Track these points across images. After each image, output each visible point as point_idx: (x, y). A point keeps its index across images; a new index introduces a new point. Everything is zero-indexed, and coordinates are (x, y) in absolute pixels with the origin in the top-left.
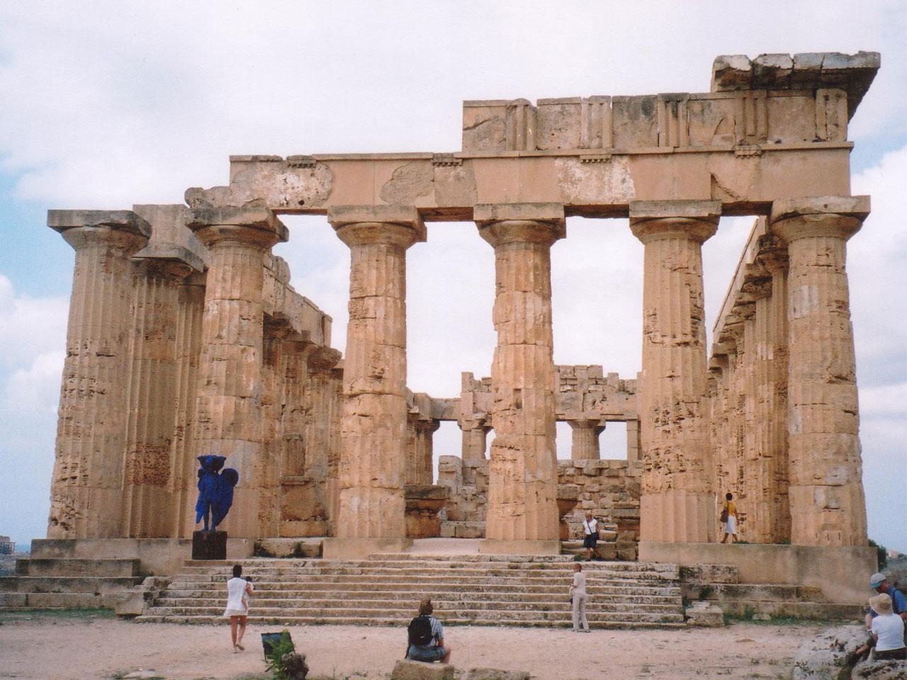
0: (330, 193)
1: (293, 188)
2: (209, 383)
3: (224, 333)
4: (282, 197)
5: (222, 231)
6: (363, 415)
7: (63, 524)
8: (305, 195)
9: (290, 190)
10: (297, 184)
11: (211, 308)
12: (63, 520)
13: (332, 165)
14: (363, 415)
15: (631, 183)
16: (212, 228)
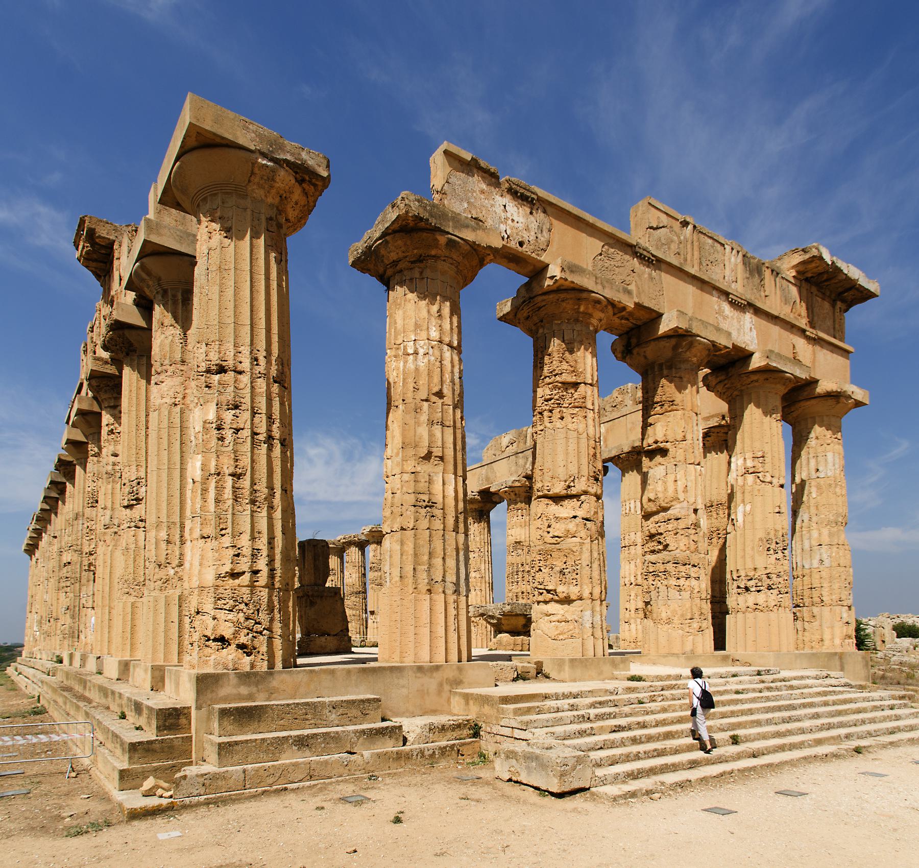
1: (513, 220)
4: (503, 227)
5: (451, 244)
6: (587, 520)
7: (241, 647)
8: (525, 236)
9: (510, 222)
12: (243, 639)
14: (587, 520)
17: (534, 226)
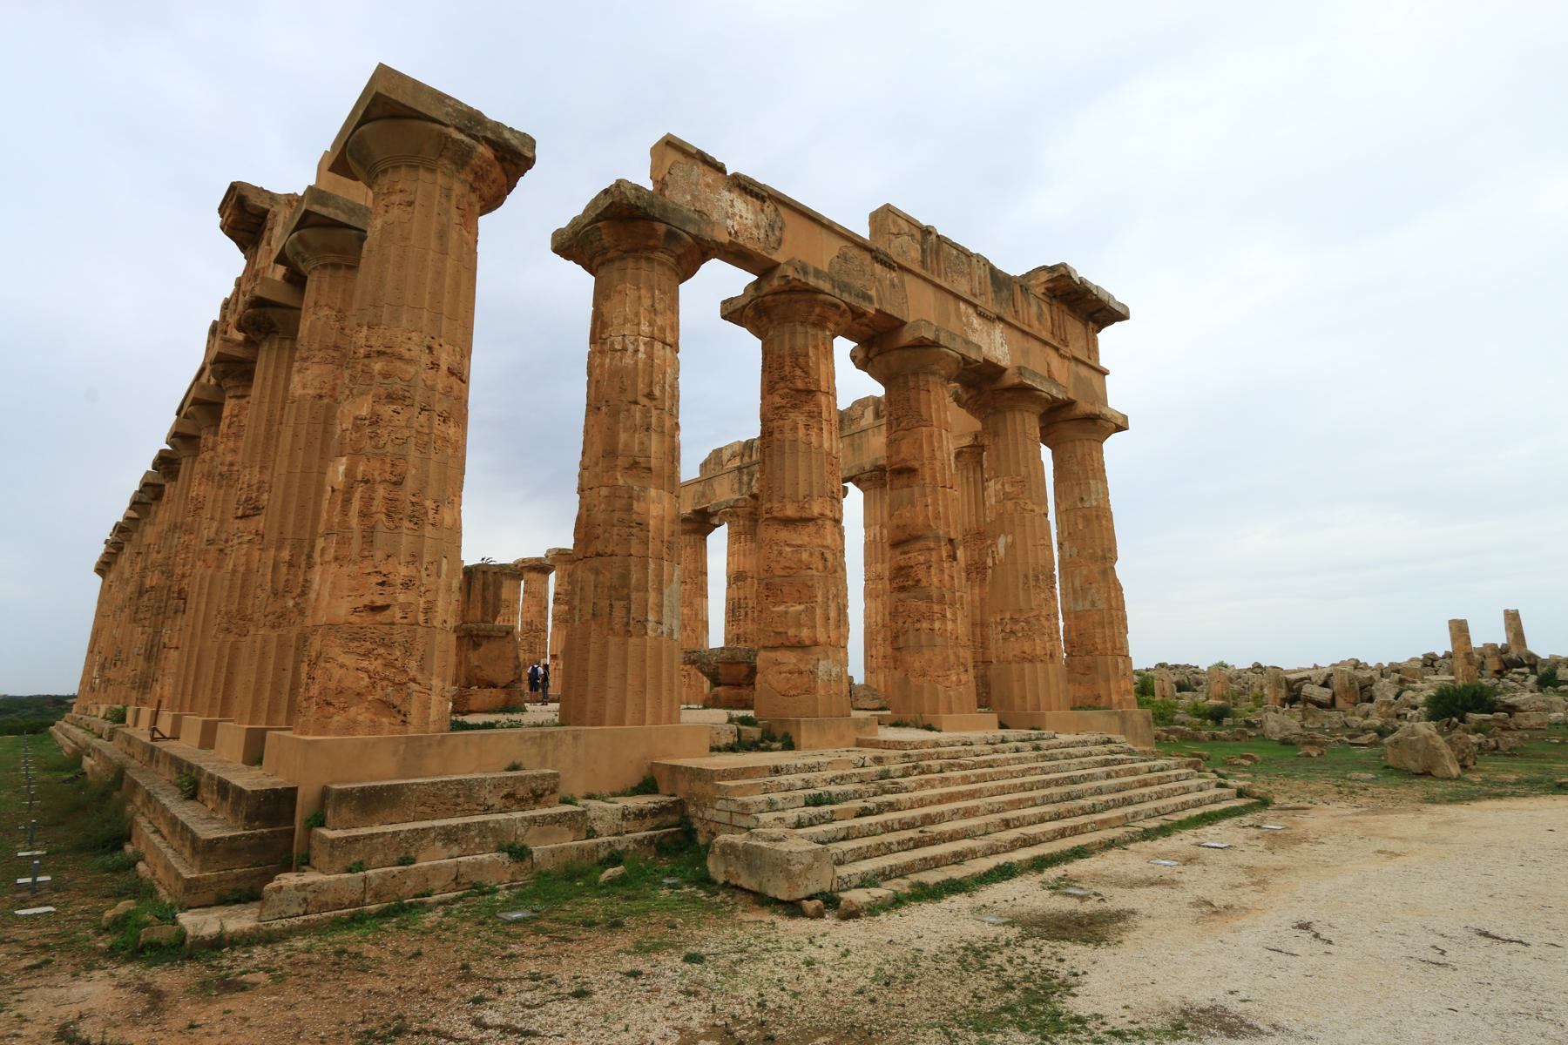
0: (780, 242)
2: (634, 465)
3: (657, 392)
4: (729, 222)
8: (755, 232)
10: (741, 216)
11: (631, 348)
13: (782, 210)
15: (1006, 348)
16: (657, 225)
17: (764, 222)
